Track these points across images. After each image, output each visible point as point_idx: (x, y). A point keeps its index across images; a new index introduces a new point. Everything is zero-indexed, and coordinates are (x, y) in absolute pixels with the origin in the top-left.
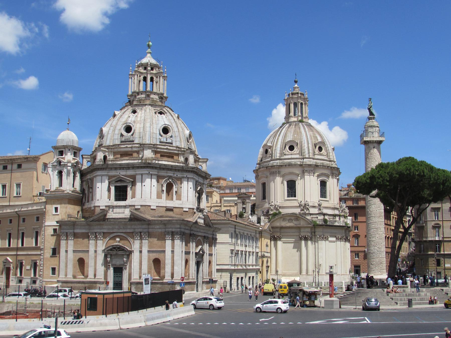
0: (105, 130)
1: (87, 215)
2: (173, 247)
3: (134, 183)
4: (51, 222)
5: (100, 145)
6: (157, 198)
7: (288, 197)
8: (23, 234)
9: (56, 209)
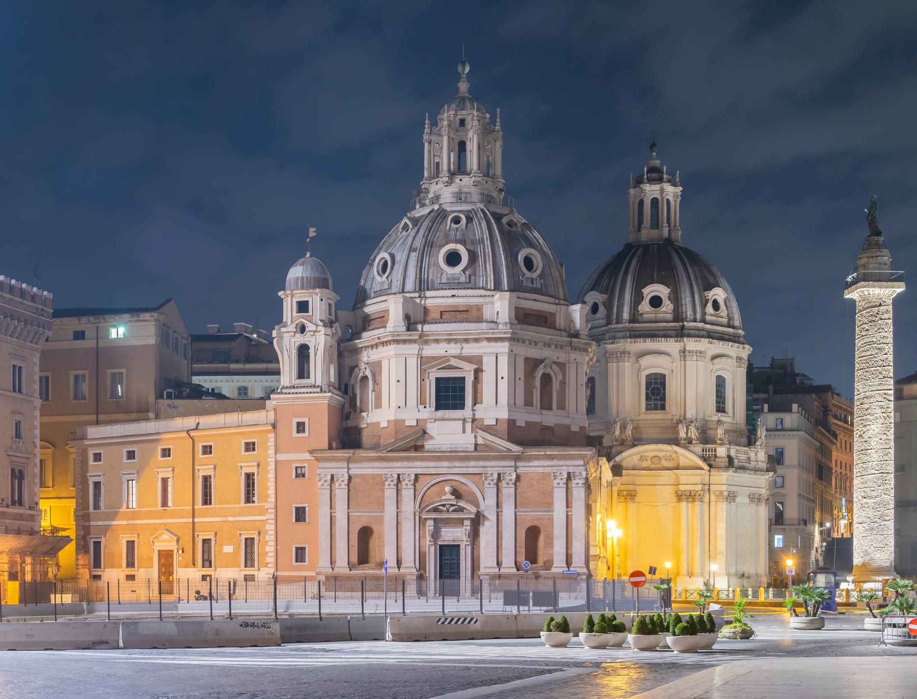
3: (478, 372)
6: (525, 405)
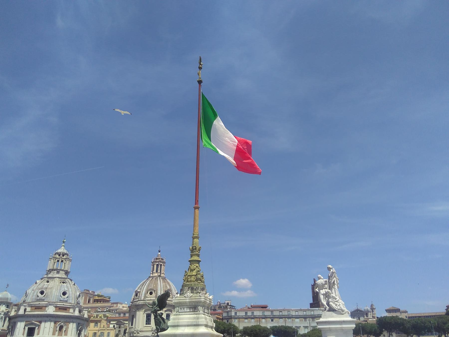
3: (39, 326)
7: (146, 324)
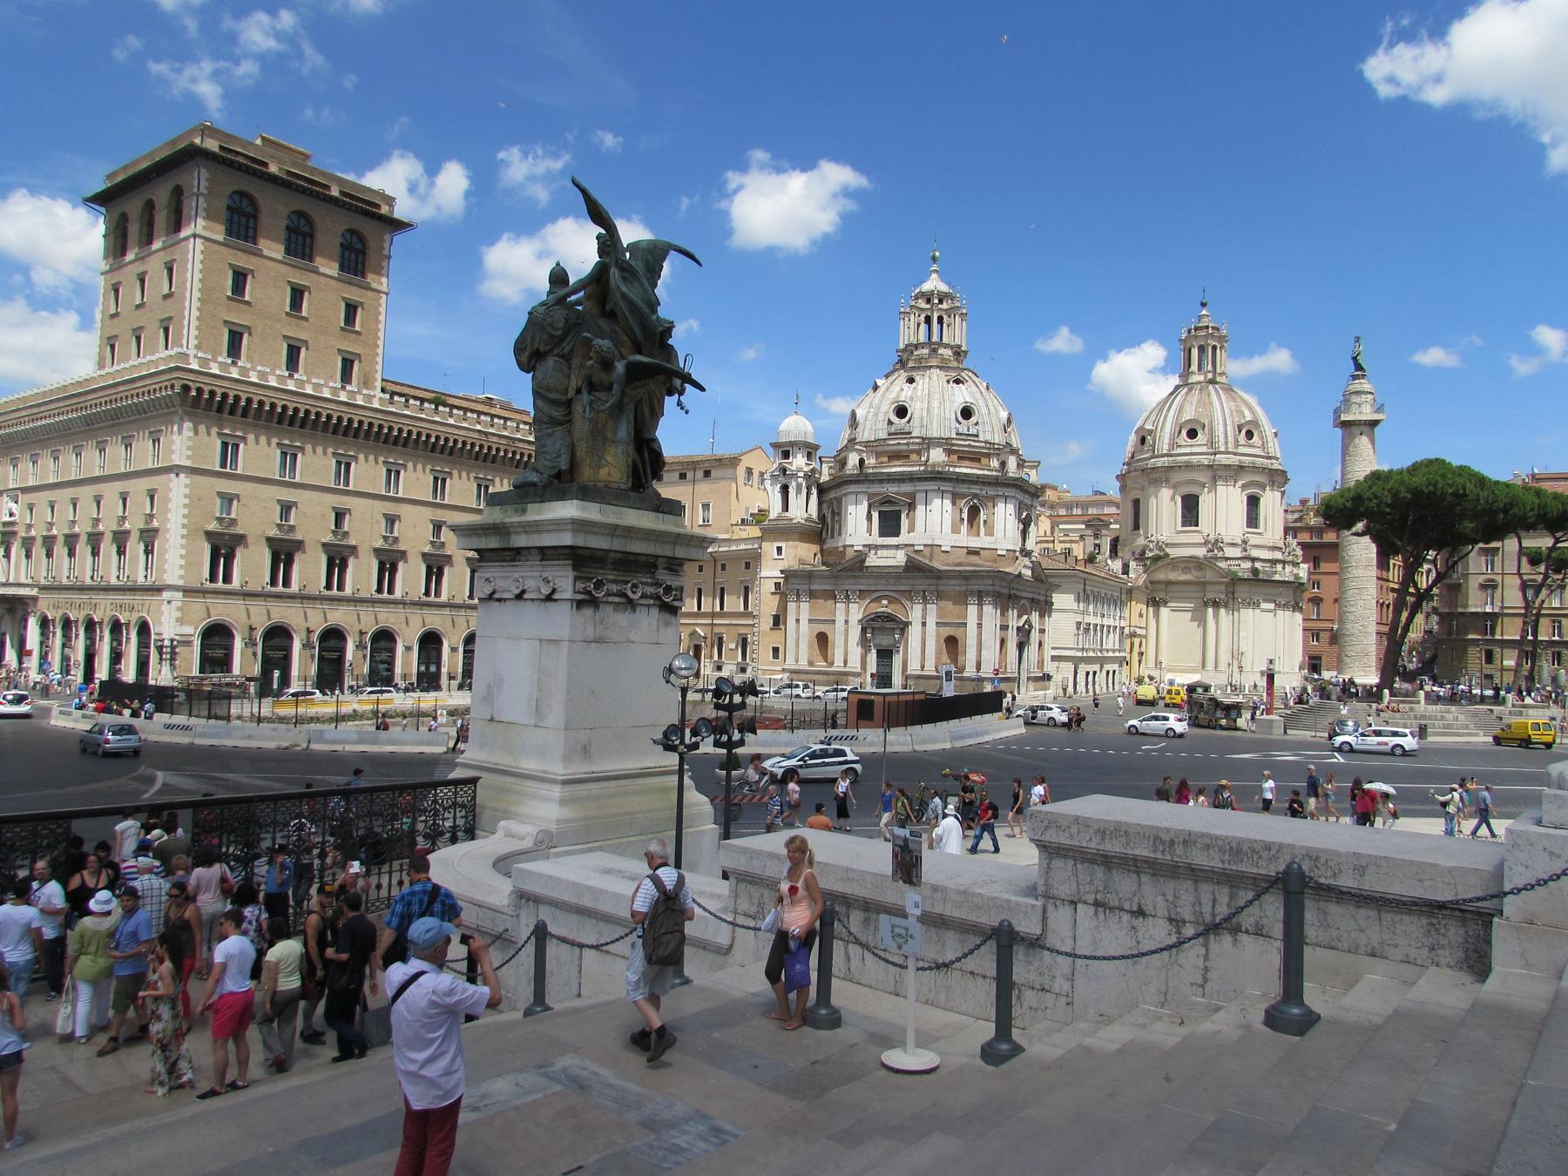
0: (860, 413)
1: (831, 559)
2: (980, 617)
3: (912, 506)
4: (770, 571)
5: (852, 441)
7: (1184, 525)
8: (722, 590)
9: (779, 549)
